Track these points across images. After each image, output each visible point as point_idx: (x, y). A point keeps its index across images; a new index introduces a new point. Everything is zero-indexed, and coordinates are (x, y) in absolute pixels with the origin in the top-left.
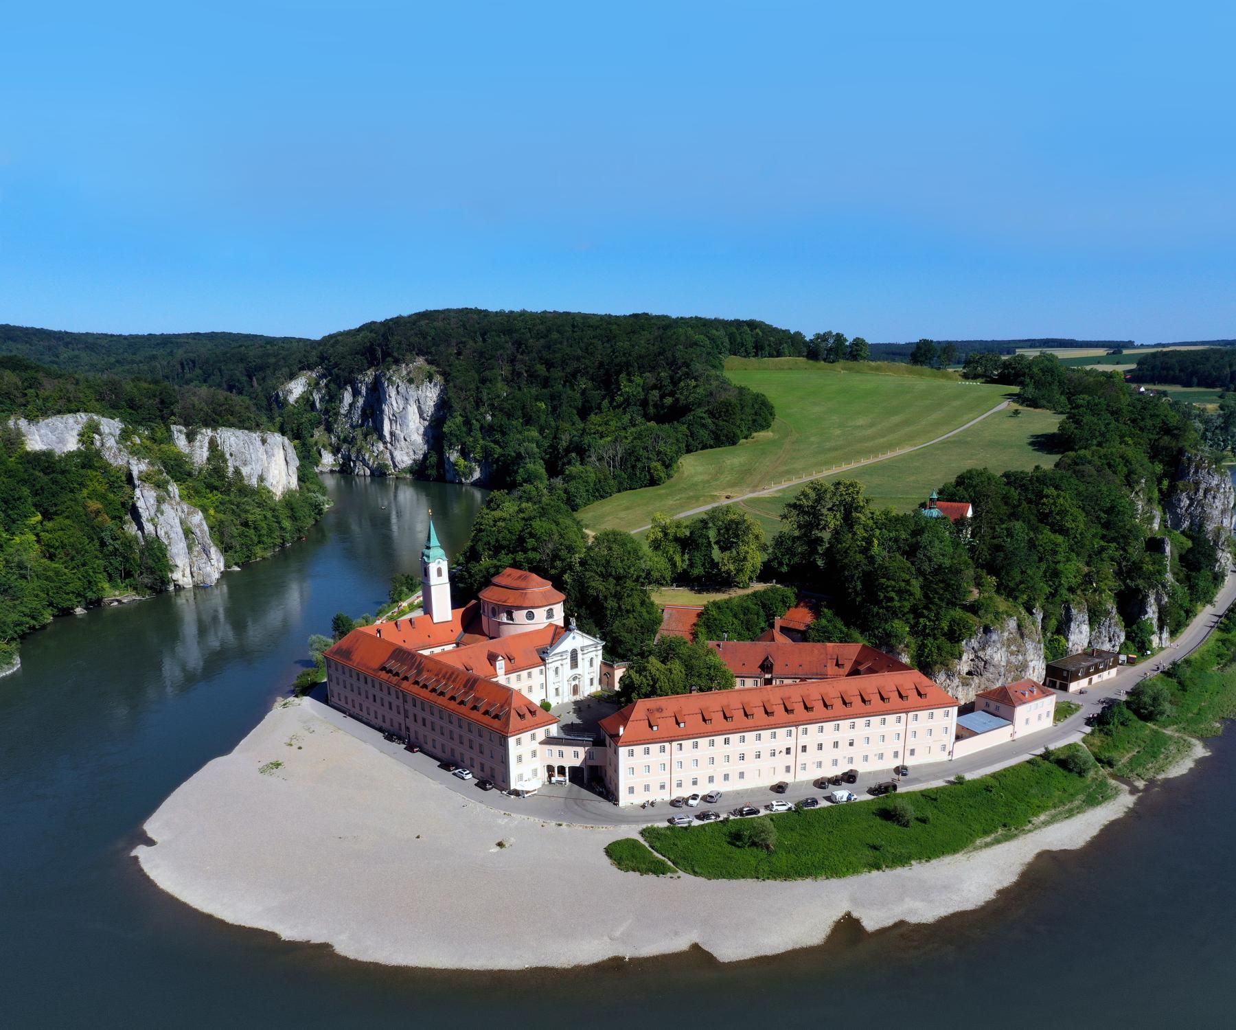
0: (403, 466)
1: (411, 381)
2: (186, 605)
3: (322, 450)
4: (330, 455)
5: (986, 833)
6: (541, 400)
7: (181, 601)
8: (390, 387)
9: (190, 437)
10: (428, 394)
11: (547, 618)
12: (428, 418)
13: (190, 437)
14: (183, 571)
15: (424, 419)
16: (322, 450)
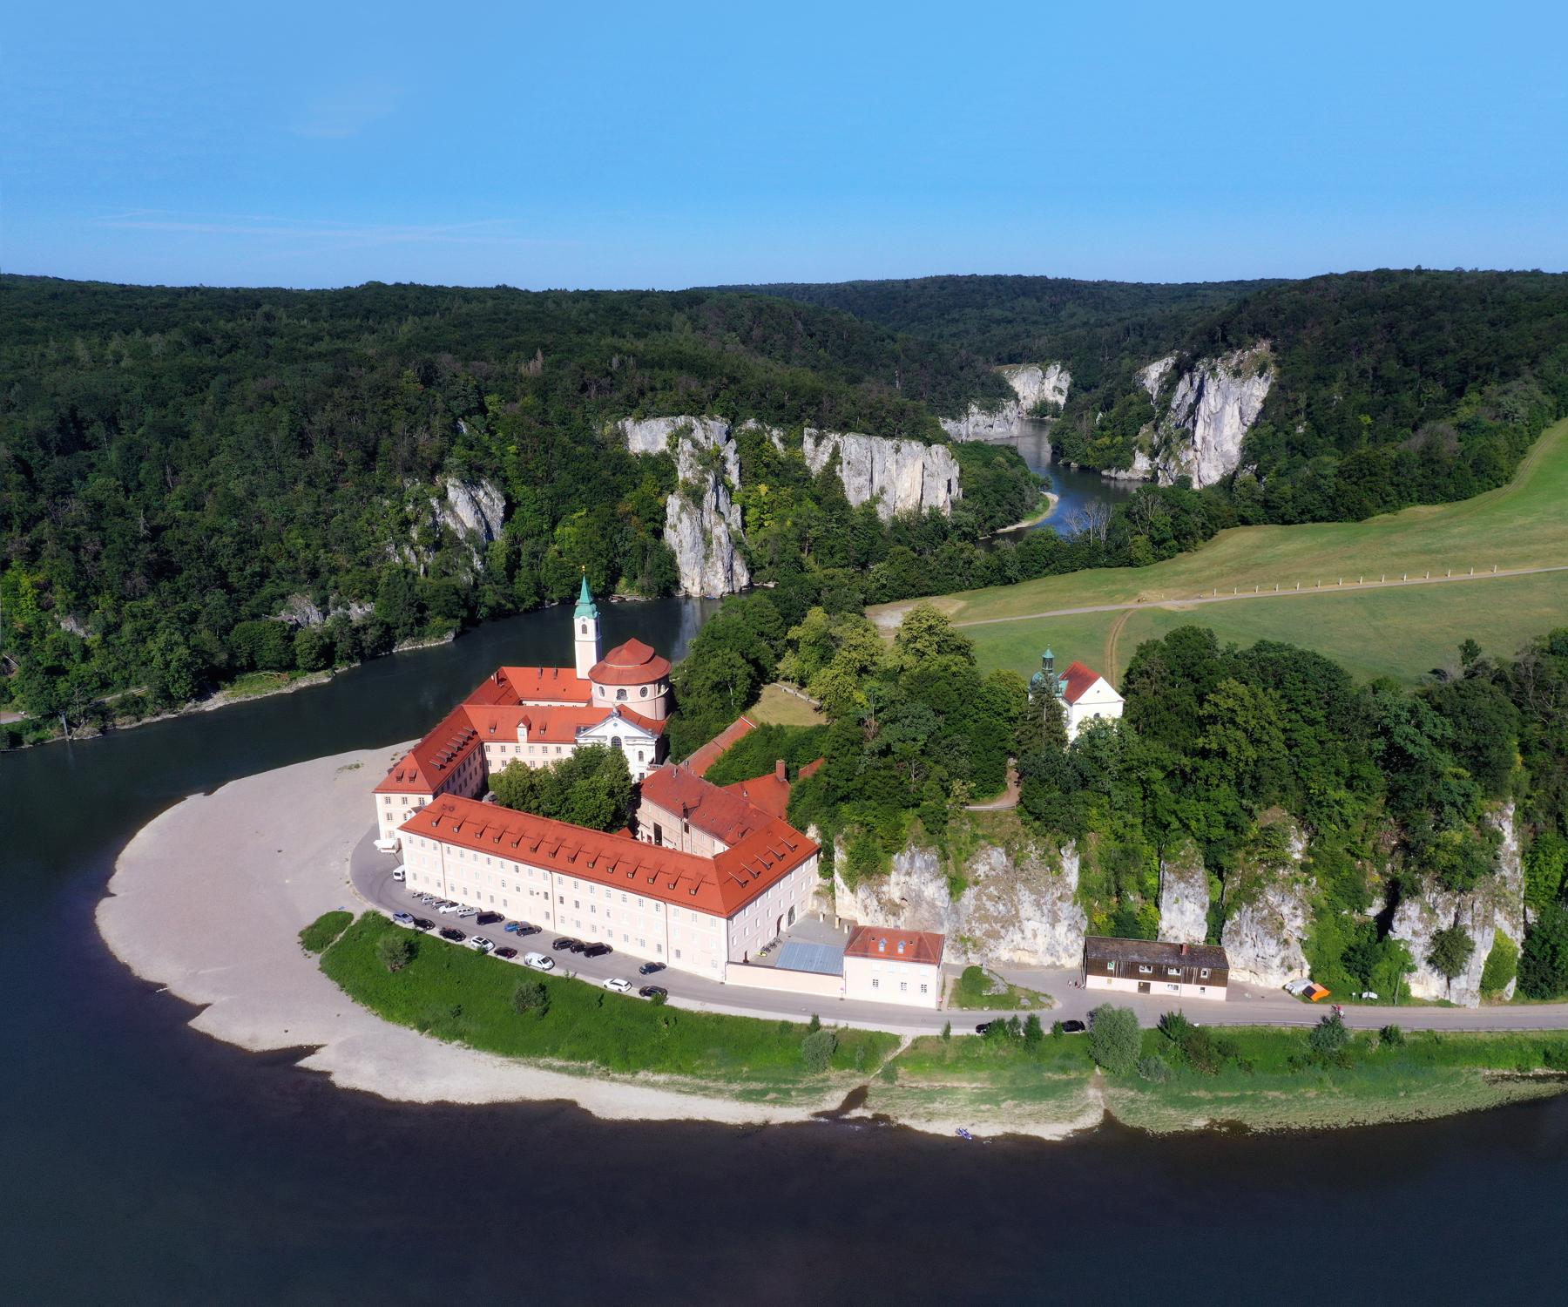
0: (1209, 482)
1: (1237, 374)
2: (692, 613)
3: (1137, 451)
4: (1146, 459)
5: (572, 1057)
6: (1365, 413)
7: (688, 609)
8: (1211, 380)
9: (818, 442)
10: (1254, 391)
11: (618, 698)
12: (1249, 424)
13: (818, 442)
14: (693, 580)
15: (1245, 425)
16: (1137, 451)
